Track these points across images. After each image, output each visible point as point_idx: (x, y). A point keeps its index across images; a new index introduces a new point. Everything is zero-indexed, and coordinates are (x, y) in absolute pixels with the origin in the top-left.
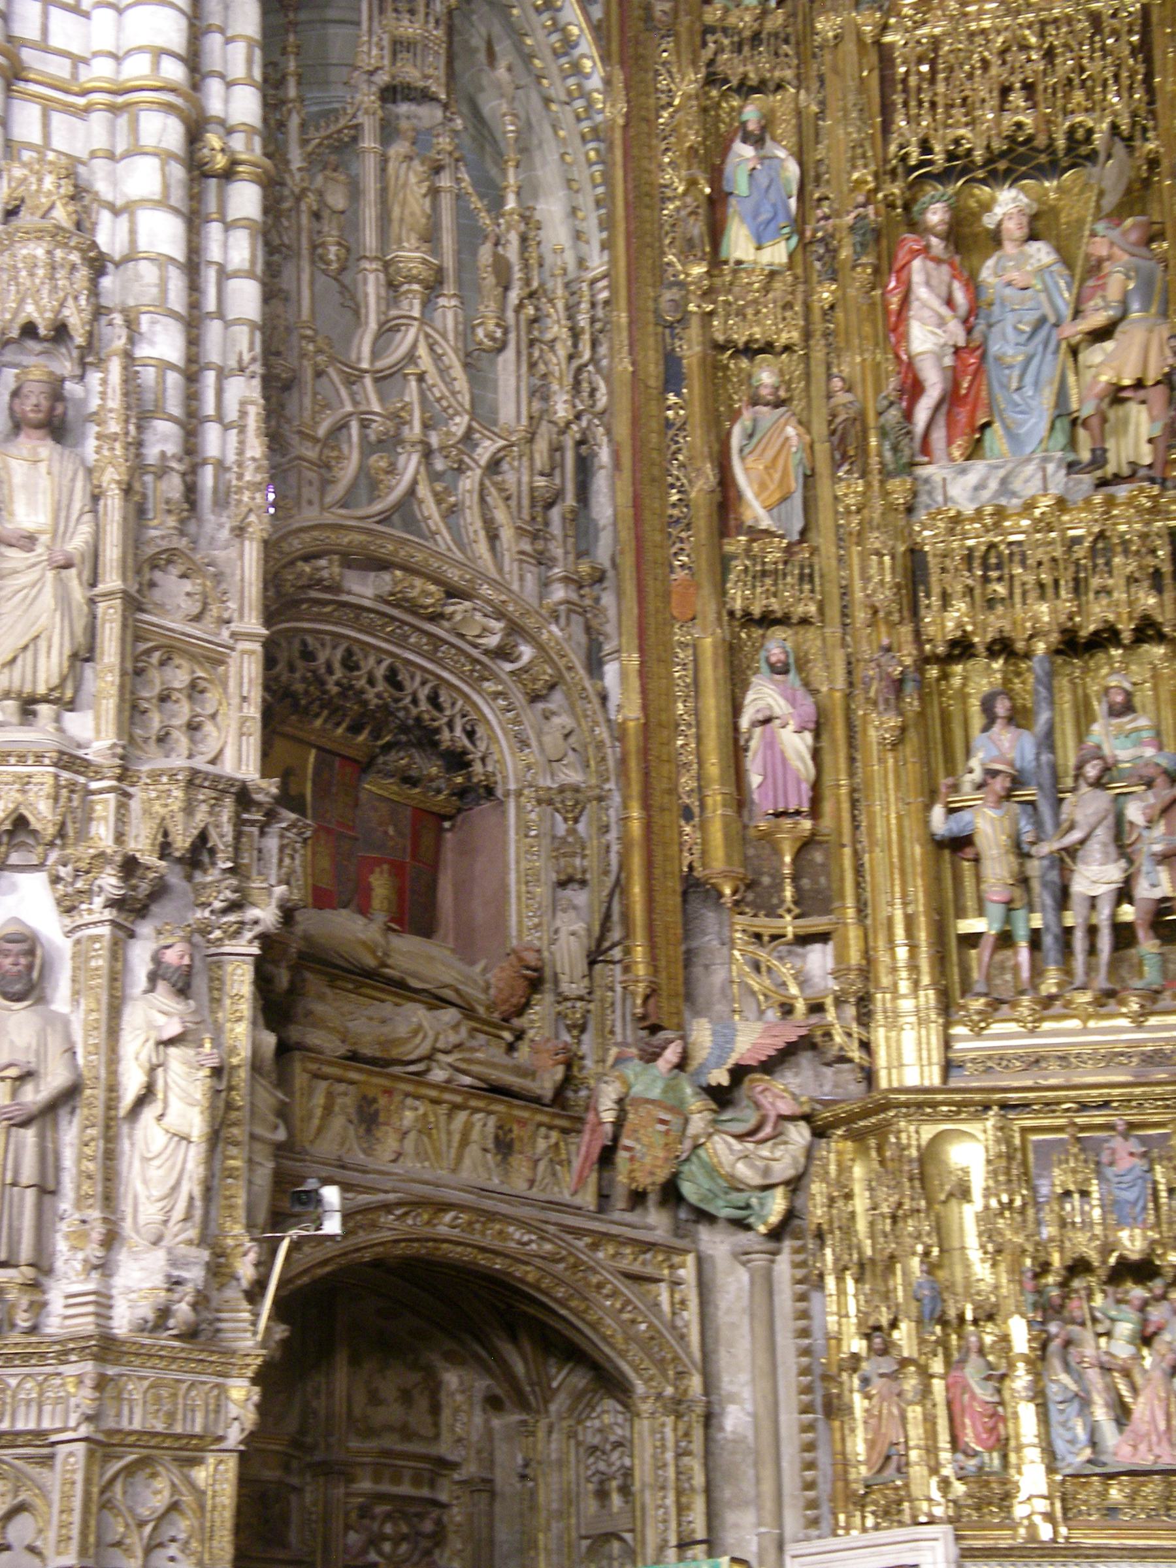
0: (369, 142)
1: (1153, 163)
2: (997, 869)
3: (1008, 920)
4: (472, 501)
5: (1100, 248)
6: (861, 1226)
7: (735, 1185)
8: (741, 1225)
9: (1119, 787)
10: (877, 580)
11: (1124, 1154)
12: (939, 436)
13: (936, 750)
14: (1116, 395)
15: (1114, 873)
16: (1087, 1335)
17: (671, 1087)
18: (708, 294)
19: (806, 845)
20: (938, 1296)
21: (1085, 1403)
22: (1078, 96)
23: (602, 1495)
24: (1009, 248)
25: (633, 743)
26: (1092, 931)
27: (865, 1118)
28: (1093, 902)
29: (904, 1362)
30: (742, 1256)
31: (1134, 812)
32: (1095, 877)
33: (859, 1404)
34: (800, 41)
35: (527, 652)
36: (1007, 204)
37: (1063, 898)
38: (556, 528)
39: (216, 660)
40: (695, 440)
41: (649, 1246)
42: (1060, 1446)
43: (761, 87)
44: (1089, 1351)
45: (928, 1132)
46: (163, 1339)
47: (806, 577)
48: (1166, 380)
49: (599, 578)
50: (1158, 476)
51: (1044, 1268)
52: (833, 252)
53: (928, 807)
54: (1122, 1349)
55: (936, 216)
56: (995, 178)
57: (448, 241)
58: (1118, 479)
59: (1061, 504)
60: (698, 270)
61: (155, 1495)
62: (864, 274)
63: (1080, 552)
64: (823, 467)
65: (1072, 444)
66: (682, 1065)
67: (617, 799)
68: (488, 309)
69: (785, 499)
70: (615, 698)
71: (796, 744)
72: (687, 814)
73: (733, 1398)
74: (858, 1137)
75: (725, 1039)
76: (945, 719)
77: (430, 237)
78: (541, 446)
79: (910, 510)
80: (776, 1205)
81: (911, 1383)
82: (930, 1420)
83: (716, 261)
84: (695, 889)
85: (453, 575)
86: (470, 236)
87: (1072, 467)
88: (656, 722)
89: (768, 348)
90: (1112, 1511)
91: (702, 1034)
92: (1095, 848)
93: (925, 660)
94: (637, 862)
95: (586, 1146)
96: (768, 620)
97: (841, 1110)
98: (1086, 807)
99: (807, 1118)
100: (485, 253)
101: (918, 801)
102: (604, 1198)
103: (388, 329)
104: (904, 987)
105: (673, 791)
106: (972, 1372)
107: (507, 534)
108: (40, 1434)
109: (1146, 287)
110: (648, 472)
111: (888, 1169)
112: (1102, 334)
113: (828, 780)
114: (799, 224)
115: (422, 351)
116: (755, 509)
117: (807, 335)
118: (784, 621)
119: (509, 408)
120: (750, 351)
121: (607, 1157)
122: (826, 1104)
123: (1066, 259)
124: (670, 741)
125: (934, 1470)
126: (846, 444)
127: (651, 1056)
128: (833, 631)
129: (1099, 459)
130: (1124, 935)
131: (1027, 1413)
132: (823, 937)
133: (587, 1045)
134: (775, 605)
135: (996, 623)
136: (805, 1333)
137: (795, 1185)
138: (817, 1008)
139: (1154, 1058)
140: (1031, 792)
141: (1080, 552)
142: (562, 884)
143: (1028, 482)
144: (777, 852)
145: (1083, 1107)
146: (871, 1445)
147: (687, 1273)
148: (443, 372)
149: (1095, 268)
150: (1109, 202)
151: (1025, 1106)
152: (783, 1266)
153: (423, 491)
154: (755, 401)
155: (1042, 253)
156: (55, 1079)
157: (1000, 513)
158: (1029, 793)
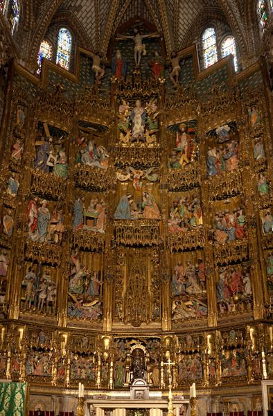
1: (65, 204)
13: (23, 272)
14: (55, 232)
15: (45, 296)
31: (49, 288)
32: (42, 296)
36: (44, 201)
48: (63, 233)
54: (36, 359)
55: (36, 199)
56: (42, 197)
109: (62, 220)
112: (55, 224)
129: (52, 240)
132: (3, 295)
139: (47, 322)
155: (47, 210)
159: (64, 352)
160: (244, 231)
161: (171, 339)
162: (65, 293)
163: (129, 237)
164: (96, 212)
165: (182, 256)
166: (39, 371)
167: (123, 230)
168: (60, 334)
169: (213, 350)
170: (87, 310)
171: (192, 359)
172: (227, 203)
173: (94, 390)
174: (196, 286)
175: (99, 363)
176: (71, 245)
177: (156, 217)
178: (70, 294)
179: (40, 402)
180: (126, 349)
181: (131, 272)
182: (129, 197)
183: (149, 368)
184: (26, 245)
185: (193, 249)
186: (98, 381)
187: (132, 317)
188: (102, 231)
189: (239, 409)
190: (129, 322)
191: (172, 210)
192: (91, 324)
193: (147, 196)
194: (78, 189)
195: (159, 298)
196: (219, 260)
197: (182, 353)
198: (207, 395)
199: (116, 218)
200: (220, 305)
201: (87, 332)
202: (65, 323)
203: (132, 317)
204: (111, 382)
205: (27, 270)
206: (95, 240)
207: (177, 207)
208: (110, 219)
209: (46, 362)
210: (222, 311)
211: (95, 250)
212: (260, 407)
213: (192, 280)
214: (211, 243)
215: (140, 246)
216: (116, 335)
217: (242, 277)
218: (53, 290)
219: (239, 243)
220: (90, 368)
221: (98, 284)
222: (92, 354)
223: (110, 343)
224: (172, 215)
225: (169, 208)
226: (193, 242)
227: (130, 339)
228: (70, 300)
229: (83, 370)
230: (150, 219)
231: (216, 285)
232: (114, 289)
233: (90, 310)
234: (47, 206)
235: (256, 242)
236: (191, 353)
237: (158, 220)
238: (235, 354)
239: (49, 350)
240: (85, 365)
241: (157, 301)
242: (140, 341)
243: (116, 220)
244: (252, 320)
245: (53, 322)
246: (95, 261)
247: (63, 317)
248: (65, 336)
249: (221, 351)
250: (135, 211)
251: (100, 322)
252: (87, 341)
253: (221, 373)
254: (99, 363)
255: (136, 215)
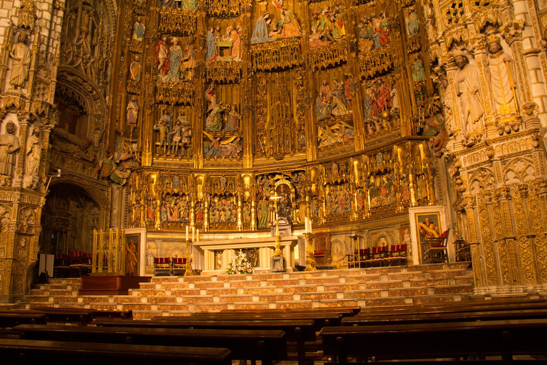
0: (80, 10)
2: (162, 136)
3: (163, 143)
4: (89, 68)
5: (187, 48)
6: (137, 186)
7: (119, 178)
8: (119, 184)
9: (181, 126)
10: (151, 90)
11: (176, 178)
12: (161, 71)
13: (156, 117)
14: (187, 69)
16: (168, 203)
17: (111, 162)
18: (130, 43)
19: (135, 128)
20: (147, 196)
21: (167, 212)
22: (187, 27)
23: (94, 221)
24: (174, 46)
25: (110, 109)
26: (175, 146)
27: (139, 170)
28: (176, 142)
29: (142, 205)
30: (118, 188)
31: (183, 130)
32: (177, 138)
33: (134, 211)
34: (148, 10)
35: (95, 93)
36: (175, 39)
37: (172, 140)
38: (101, 74)
39: (48, 84)
40: (125, 64)
41: (105, 186)
42: (162, 218)
43: (141, 15)
44: (168, 205)
45: (148, 173)
46: (31, 190)
47: (139, 88)
48: (195, 69)
49: (107, 83)
50: (192, 82)
51: (163, 193)
52: (149, 41)
53: (154, 125)
54: (172, 205)
55: (165, 39)
56: (173, 36)
57: (90, 27)
58: (186, 81)
59: (178, 83)
60: (129, 39)
61: (28, 213)
62: (153, 45)
63: (180, 91)
64: (144, 72)
65: (180, 75)
66: (112, 159)
67: (106, 117)
68: (95, 39)
69: (138, 76)
70: (107, 102)
71: (135, 113)
72: (117, 121)
73: (115, 209)
74: (138, 173)
75: (119, 156)
76: (157, 113)
77: (88, 27)
78: (101, 61)
79: (156, 81)
80: (125, 181)
81: (142, 208)
82: (144, 214)
83: (131, 39)
84: (117, 133)
85: (85, 79)
86: (94, 27)
87: (180, 79)
88: (114, 107)
89: (138, 53)
90: (168, 227)
91: (116, 155)
92: (177, 134)
93: (155, 103)
94: (109, 127)
95: (96, 170)
96: (133, 94)
97: (136, 168)
98: (177, 128)
99: (130, 169)
100: (96, 30)
101: (152, 124)
102: (98, 178)
103: (79, 39)
104: (147, 151)
105: (115, 117)
106: (151, 207)
107: (94, 74)
108: (11, 202)
109: (193, 55)
110: (117, 69)
111: (142, 178)
112: (187, 60)
113: (139, 119)
114: (144, 36)
115: (84, 43)
116: (133, 76)
117: (144, 52)
118: (135, 94)
119: (96, 55)
120: (135, 53)
121: (99, 172)
122: (134, 167)
123: (182, 49)
124: (116, 110)
125: (144, 220)
126: (147, 69)
127: (108, 157)
128: (142, 97)
129: (184, 78)
130: (180, 147)
131: (158, 213)
132: (136, 143)
133: (98, 155)
134: (134, 91)
135: (167, 99)
136: (127, 200)
137: (128, 179)
138: (134, 153)
139: (182, 165)
140: (169, 125)
141: (180, 91)
142: (96, 129)
143: (174, 80)
144: (130, 129)
145: (171, 171)
146: (135, 217)
147: (110, 190)
148: (87, 47)
149: (186, 51)
150: (189, 42)
151: (163, 170)
152: (124, 190)
153: (82, 65)
154: (135, 60)
155: (179, 47)
156: (16, 147)
157: (169, 83)
158: (168, 125)
159: (201, 195)
160: (388, 35)
161: (316, 170)
162: (200, 133)
163: (267, 61)
164: (231, 40)
165: (329, 75)
166: (175, 218)
167: (260, 54)
168: (197, 177)
169: (361, 178)
170: (225, 148)
171: (341, 190)
172: (373, 6)
173: (234, 232)
174: (341, 106)
175: (240, 203)
176: (204, 81)
177: (297, 35)
178: (205, 133)
179: (177, 248)
180: (270, 186)
181: (273, 100)
182: (266, 17)
183: (294, 205)
184: (156, 87)
185: (337, 65)
186: (239, 223)
187: (273, 150)
188: (237, 59)
189: (388, 244)
190: (272, 155)
191: (313, 23)
192: (230, 162)
193: (286, 12)
194: (213, 19)
195: (304, 124)
196: (363, 74)
197: (328, 184)
198: (354, 230)
199: (252, 43)
200: (369, 125)
201: (224, 171)
202: (201, 164)
203: (273, 150)
204: (253, 223)
205: (162, 114)
206: (231, 70)
207: (317, 19)
208: (248, 45)
209: (183, 207)
210: (370, 132)
211: (231, 82)
212: (409, 238)
213: (336, 100)
214: (354, 55)
215: (279, 70)
216: (257, 171)
217: (390, 90)
218: (188, 130)
219: (382, 51)
220: (230, 210)
221: (236, 119)
222: (231, 195)
223: (251, 180)
224: (314, 30)
225: (310, 21)
226: (336, 57)
227: (273, 175)
228: (206, 139)
229: (222, 212)
230: (290, 38)
231: (362, 102)
232: (254, 122)
233: (229, 148)
234: (179, 43)
235: (401, 46)
236: (336, 183)
237: (299, 38)
238: (384, 179)
239: (184, 195)
240: (225, 207)
241: (303, 128)
242: (285, 175)
243: (253, 45)
244: (399, 137)
245: (188, 165)
246: (235, 95)
247: (198, 158)
248: (202, 177)
249: (369, 178)
250: (274, 31)
251: (239, 160)
252: (225, 181)
253: (370, 203)
254: (240, 203)
255: (275, 35)
